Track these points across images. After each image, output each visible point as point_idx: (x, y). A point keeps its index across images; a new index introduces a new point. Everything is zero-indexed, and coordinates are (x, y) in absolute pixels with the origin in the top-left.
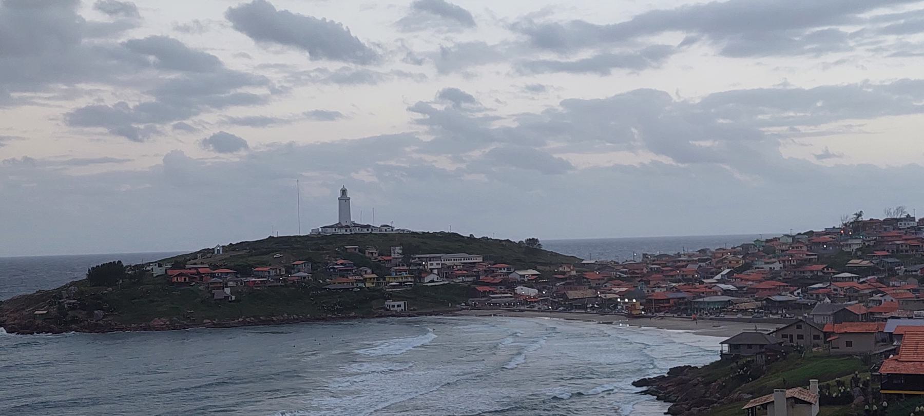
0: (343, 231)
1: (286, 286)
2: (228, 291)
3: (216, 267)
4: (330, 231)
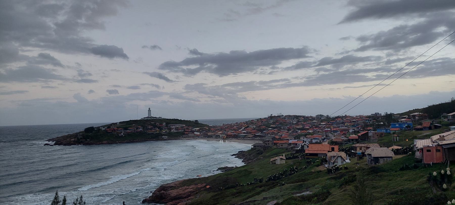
2: (122, 134)
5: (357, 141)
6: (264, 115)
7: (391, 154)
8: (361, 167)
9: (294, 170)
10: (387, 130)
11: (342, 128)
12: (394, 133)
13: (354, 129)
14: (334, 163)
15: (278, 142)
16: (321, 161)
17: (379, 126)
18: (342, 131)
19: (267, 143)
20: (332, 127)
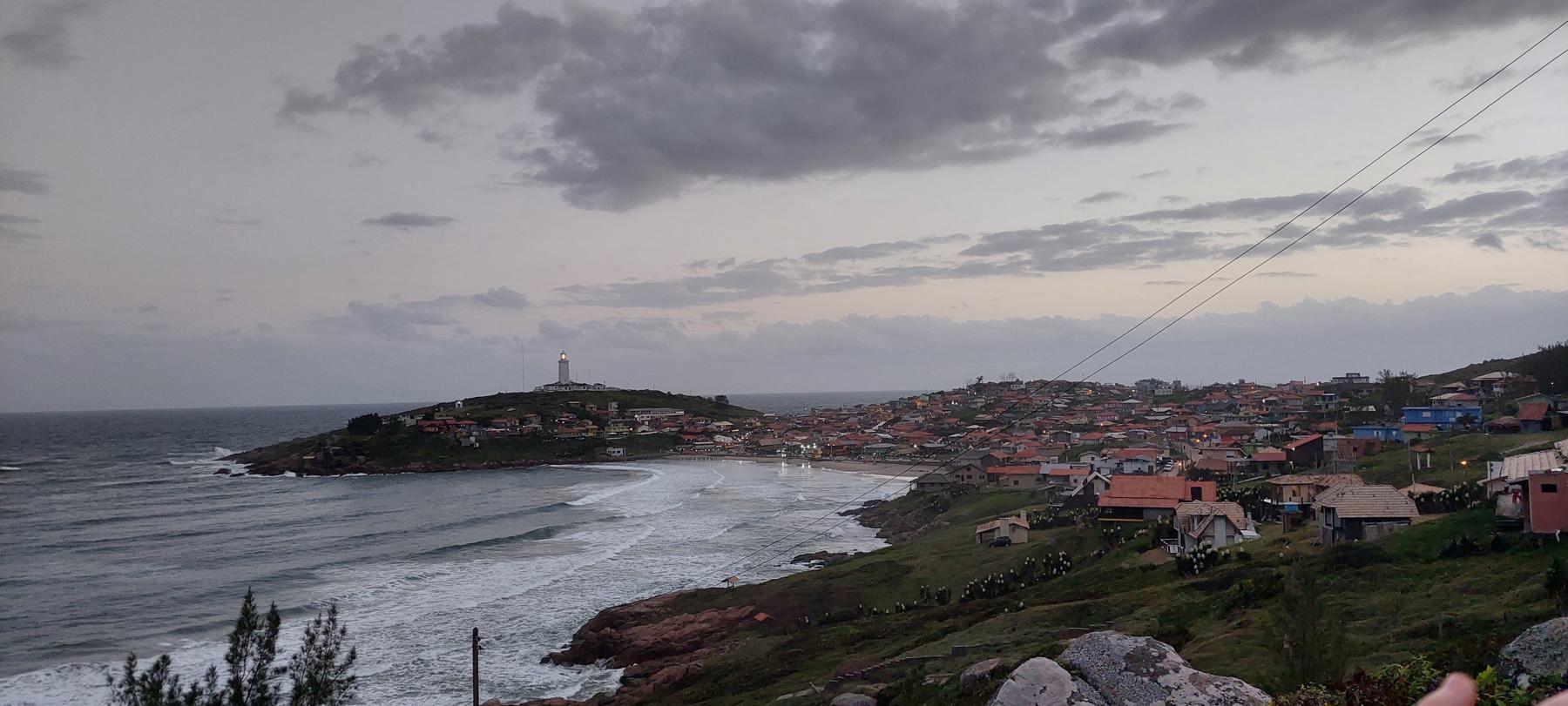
2: (473, 439)
3: (459, 419)
5: (1282, 468)
6: (953, 377)
7: (1408, 510)
8: (1297, 553)
9: (1058, 565)
10: (1388, 431)
11: (1230, 424)
12: (1414, 442)
13: (1271, 429)
14: (1199, 540)
15: (999, 470)
16: (1152, 534)
17: (1362, 419)
18: (1227, 434)
19: (965, 473)
20: (1192, 422)
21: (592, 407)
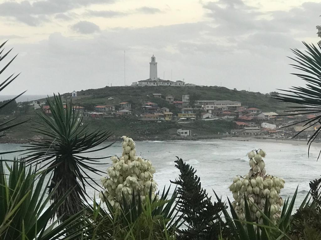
0: (152, 84)
1: (115, 118)
4: (144, 84)
21: (170, 98)
